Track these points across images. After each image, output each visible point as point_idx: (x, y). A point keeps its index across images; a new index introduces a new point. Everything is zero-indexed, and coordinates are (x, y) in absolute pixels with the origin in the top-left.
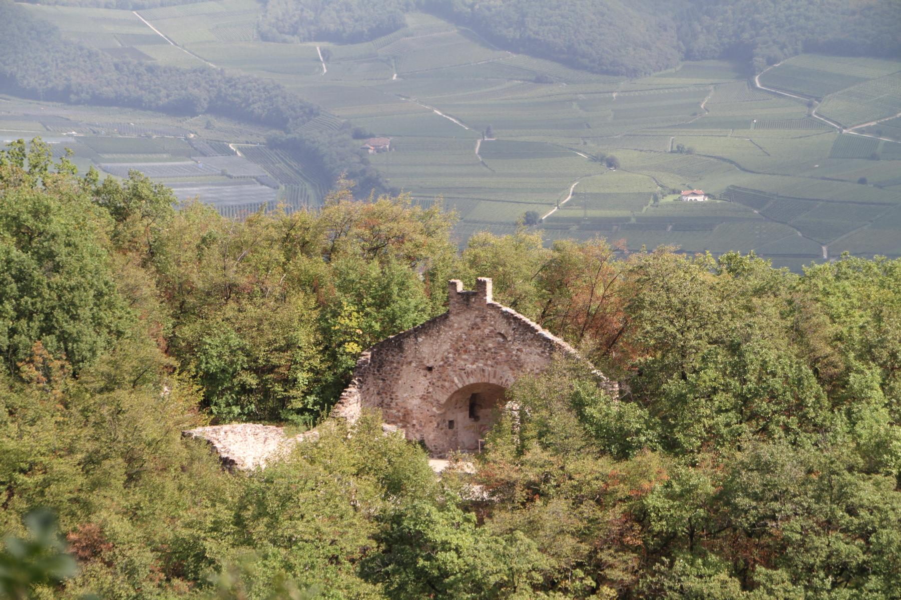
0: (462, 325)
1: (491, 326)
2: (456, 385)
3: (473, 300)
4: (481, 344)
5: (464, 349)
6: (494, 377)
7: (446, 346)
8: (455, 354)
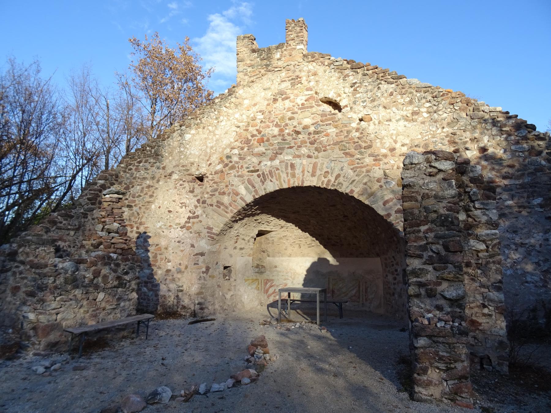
0: (257, 99)
2: (242, 199)
3: (278, 56)
5: (259, 136)
6: (313, 175)
8: (242, 149)
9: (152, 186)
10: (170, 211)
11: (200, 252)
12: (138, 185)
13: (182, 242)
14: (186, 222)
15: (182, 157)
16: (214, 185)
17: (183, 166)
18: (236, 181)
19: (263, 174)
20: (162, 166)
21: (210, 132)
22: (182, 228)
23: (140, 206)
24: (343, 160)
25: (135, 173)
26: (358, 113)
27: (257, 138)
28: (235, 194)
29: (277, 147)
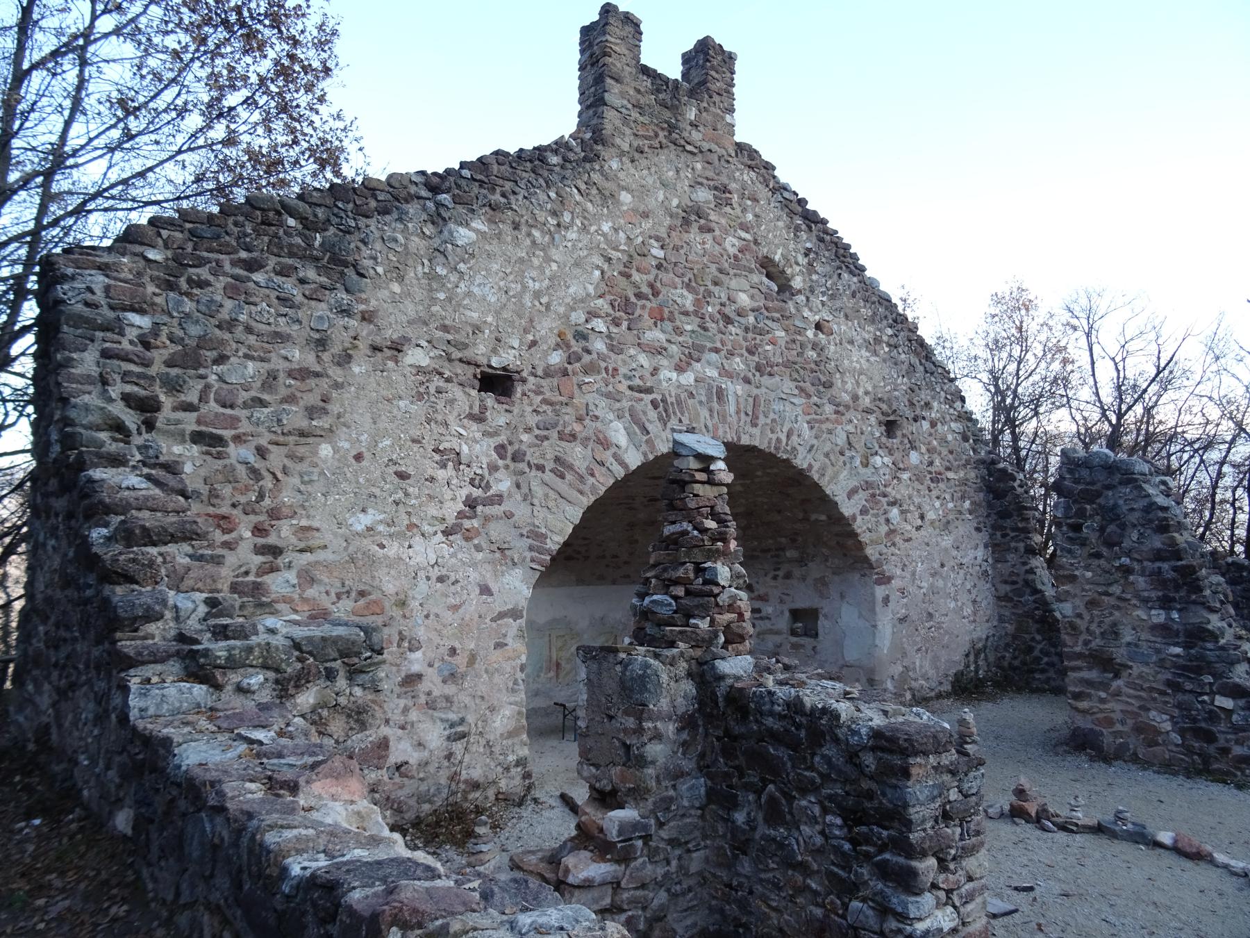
0: (652, 203)
1: (745, 227)
4: (716, 290)
7: (584, 284)
9: (317, 375)
10: (402, 476)
11: (510, 607)
12: (246, 356)
13: (453, 579)
14: (461, 515)
15: (442, 296)
16: (545, 407)
17: (445, 329)
18: (602, 408)
19: (664, 401)
20: (362, 307)
21: (534, 242)
22: (447, 533)
23: (263, 442)
24: (795, 400)
25: (229, 304)
26: (816, 313)
27: (648, 304)
28: (599, 442)
29: (690, 341)
